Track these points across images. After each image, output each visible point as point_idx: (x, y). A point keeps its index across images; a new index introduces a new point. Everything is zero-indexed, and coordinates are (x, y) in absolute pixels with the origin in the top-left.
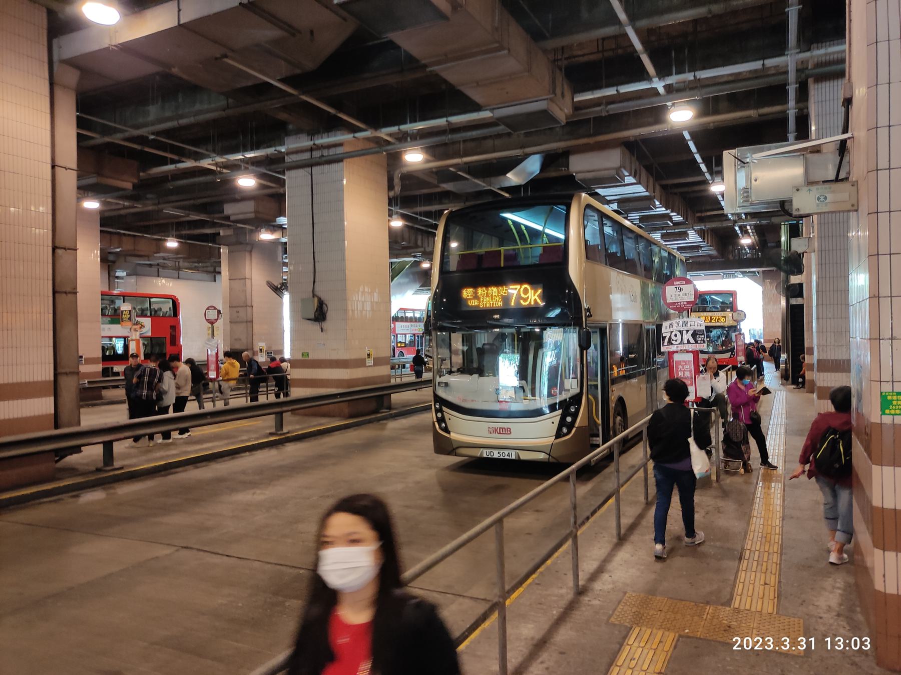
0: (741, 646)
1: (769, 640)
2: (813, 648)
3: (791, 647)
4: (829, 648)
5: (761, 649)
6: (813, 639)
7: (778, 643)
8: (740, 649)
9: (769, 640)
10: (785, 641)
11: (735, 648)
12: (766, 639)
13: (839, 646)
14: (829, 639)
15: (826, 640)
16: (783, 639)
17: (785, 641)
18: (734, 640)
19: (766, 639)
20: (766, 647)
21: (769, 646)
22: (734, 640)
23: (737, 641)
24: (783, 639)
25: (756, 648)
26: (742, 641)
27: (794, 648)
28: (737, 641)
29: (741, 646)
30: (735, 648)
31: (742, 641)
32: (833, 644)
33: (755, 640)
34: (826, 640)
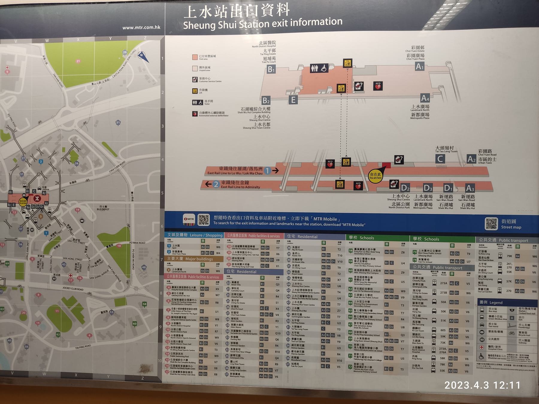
0: (450, 386)
1: (467, 383)
2: (512, 388)
3: (470, 388)
4: (496, 388)
5: (462, 388)
6: (518, 383)
7: (472, 384)
10: (486, 383)
11: (446, 388)
12: (465, 383)
14: (496, 383)
15: (494, 383)
16: (485, 383)
17: (486, 383)
18: (445, 383)
19: (465, 383)
20: (465, 387)
21: (467, 387)
22: (445, 383)
23: (447, 383)
24: (485, 383)
25: (459, 388)
26: (450, 384)
27: (481, 388)
28: (447, 383)
29: (450, 386)
30: (446, 388)
32: (499, 385)
33: (458, 383)
34: (494, 383)
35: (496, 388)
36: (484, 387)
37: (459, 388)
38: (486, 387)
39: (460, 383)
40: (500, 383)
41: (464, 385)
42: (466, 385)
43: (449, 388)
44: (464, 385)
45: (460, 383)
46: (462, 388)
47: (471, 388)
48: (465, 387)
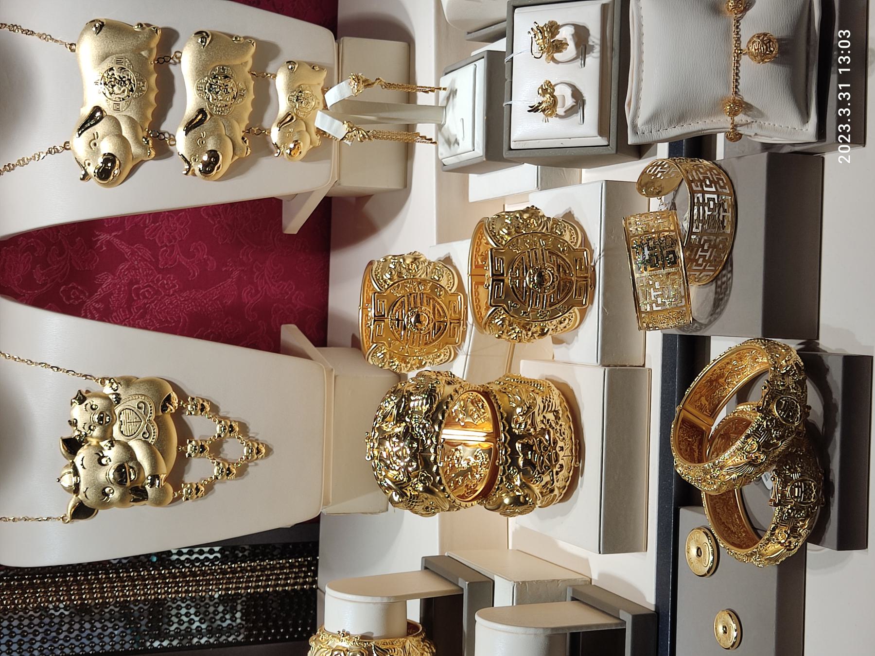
1: (842, 128)
2: (849, 85)
4: (849, 70)
5: (849, 135)
6: (840, 86)
8: (849, 156)
9: (842, 128)
10: (842, 112)
11: (849, 162)
12: (840, 131)
13: (847, 60)
14: (840, 70)
15: (841, 73)
18: (841, 162)
19: (840, 131)
20: (848, 131)
21: (847, 128)
22: (841, 162)
23: (841, 159)
25: (849, 141)
26: (842, 154)
27: (849, 104)
28: (841, 159)
30: (849, 162)
31: (842, 154)
32: (844, 65)
33: (841, 141)
34: (841, 73)
35: (849, 70)
36: (848, 115)
37: (849, 141)
38: (847, 96)
39: (842, 139)
40: (840, 63)
41: (844, 132)
42: (844, 129)
43: (849, 156)
44: (844, 132)
45: (842, 139)
46: (849, 135)
47: (849, 52)
48: (848, 131)
